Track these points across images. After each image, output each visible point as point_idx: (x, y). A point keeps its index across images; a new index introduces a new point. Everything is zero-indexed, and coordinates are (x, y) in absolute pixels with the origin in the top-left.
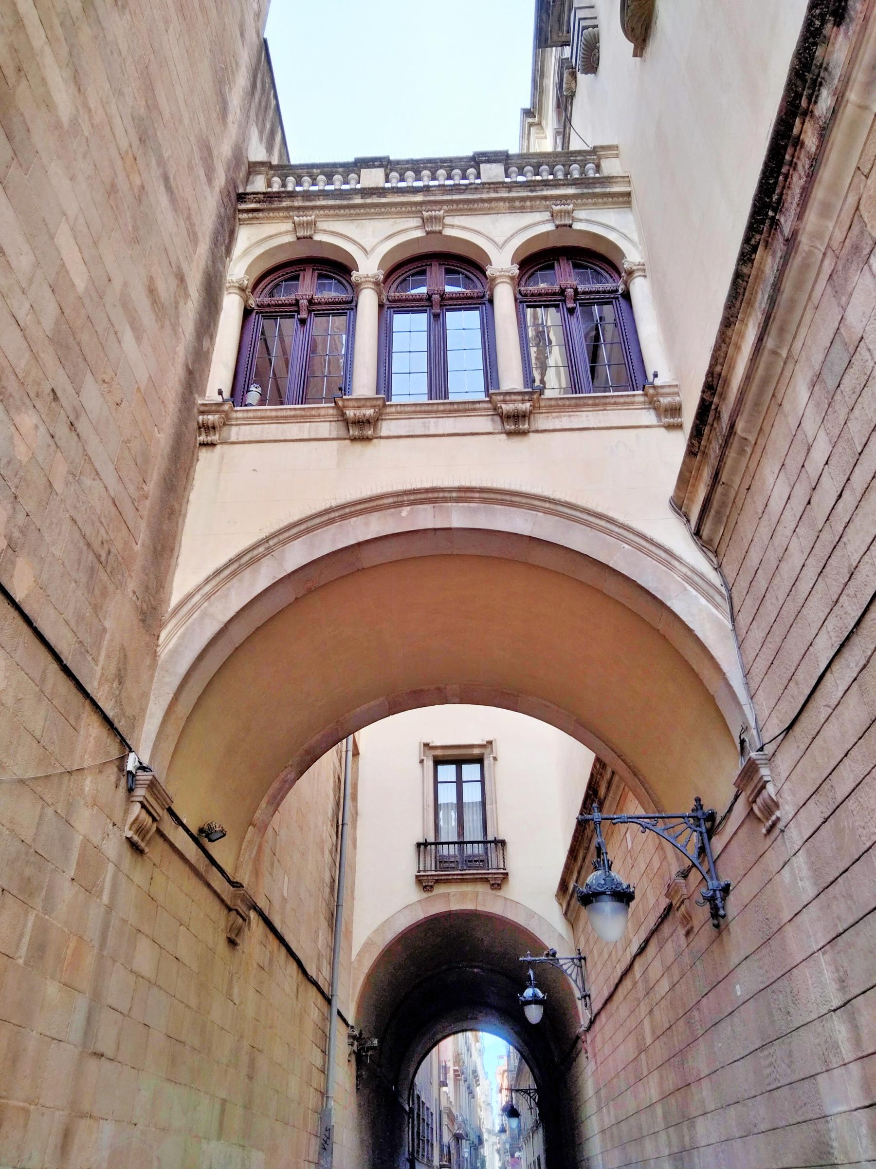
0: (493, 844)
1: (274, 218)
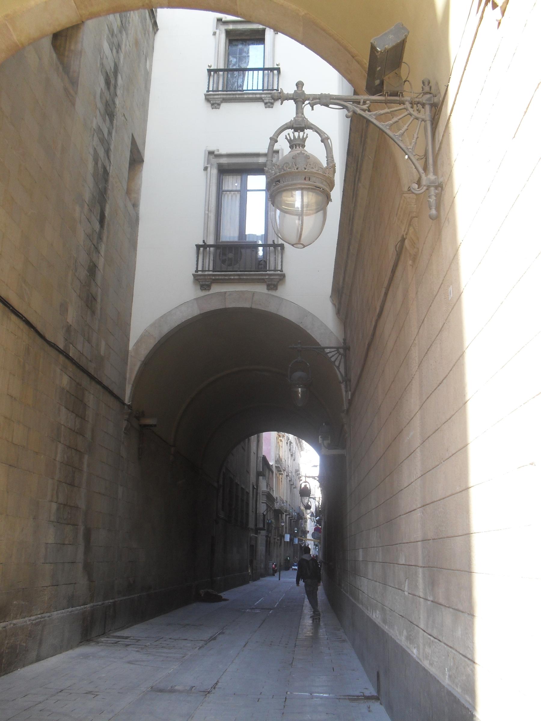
0: (272, 248)
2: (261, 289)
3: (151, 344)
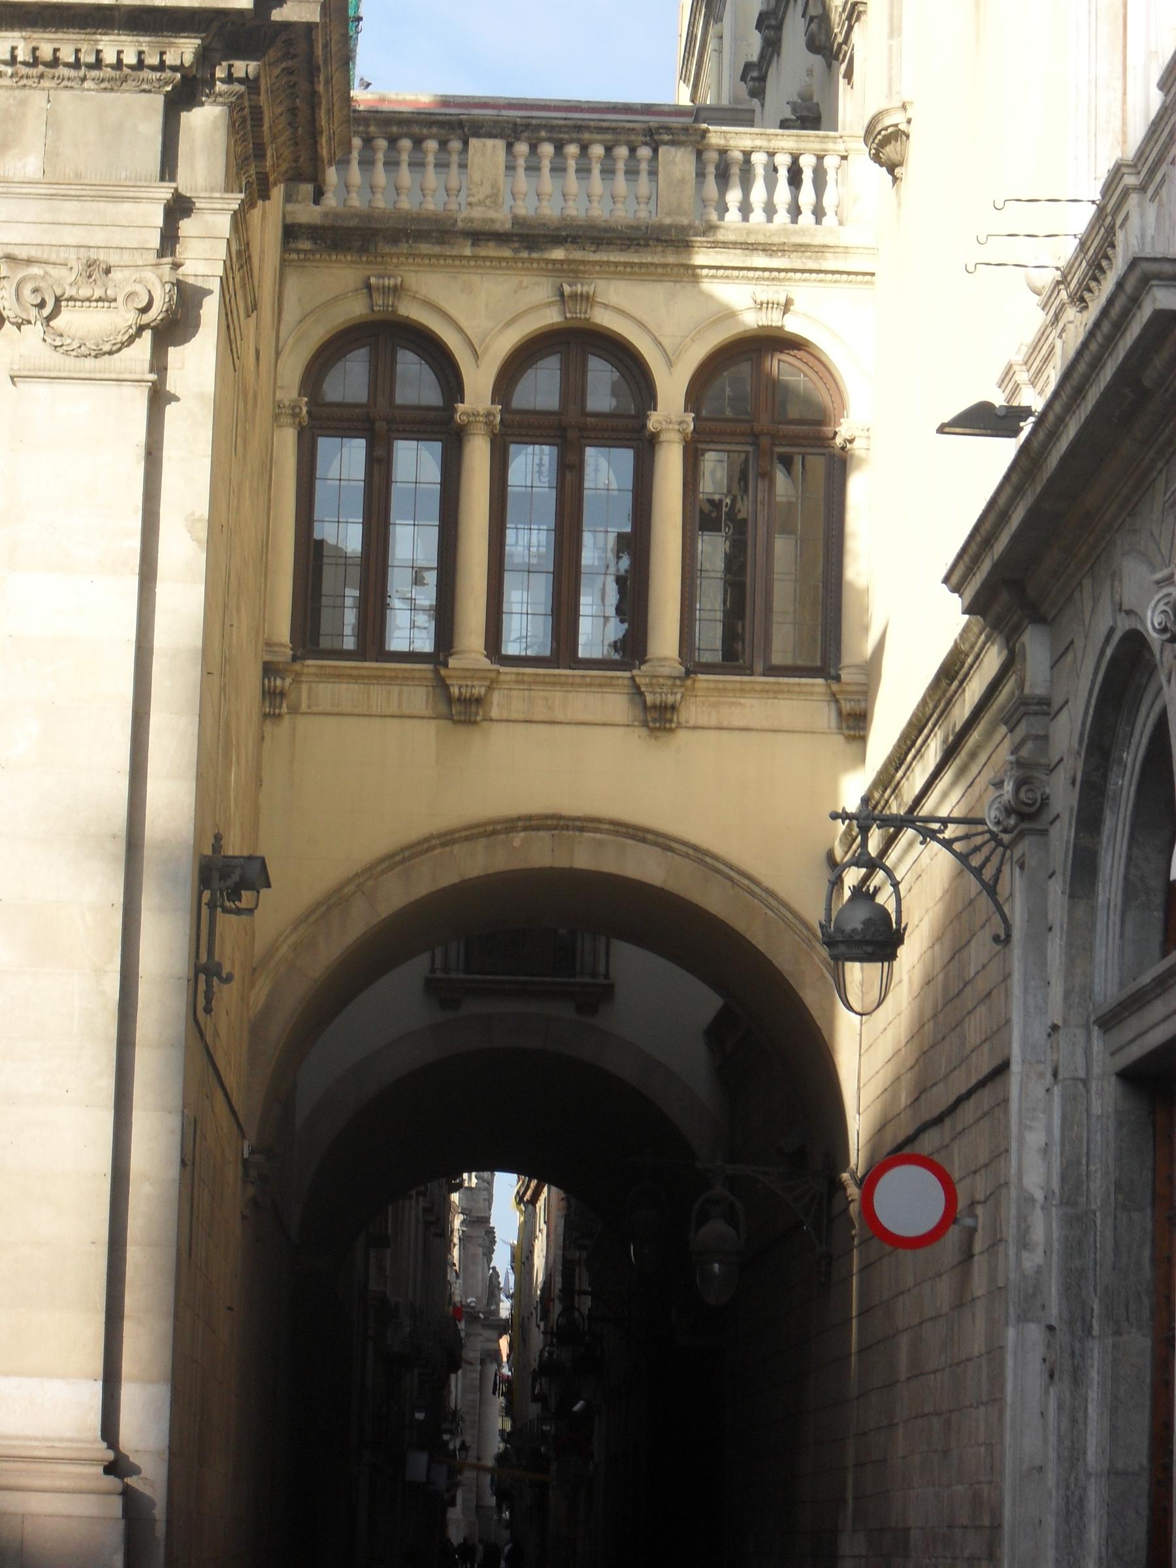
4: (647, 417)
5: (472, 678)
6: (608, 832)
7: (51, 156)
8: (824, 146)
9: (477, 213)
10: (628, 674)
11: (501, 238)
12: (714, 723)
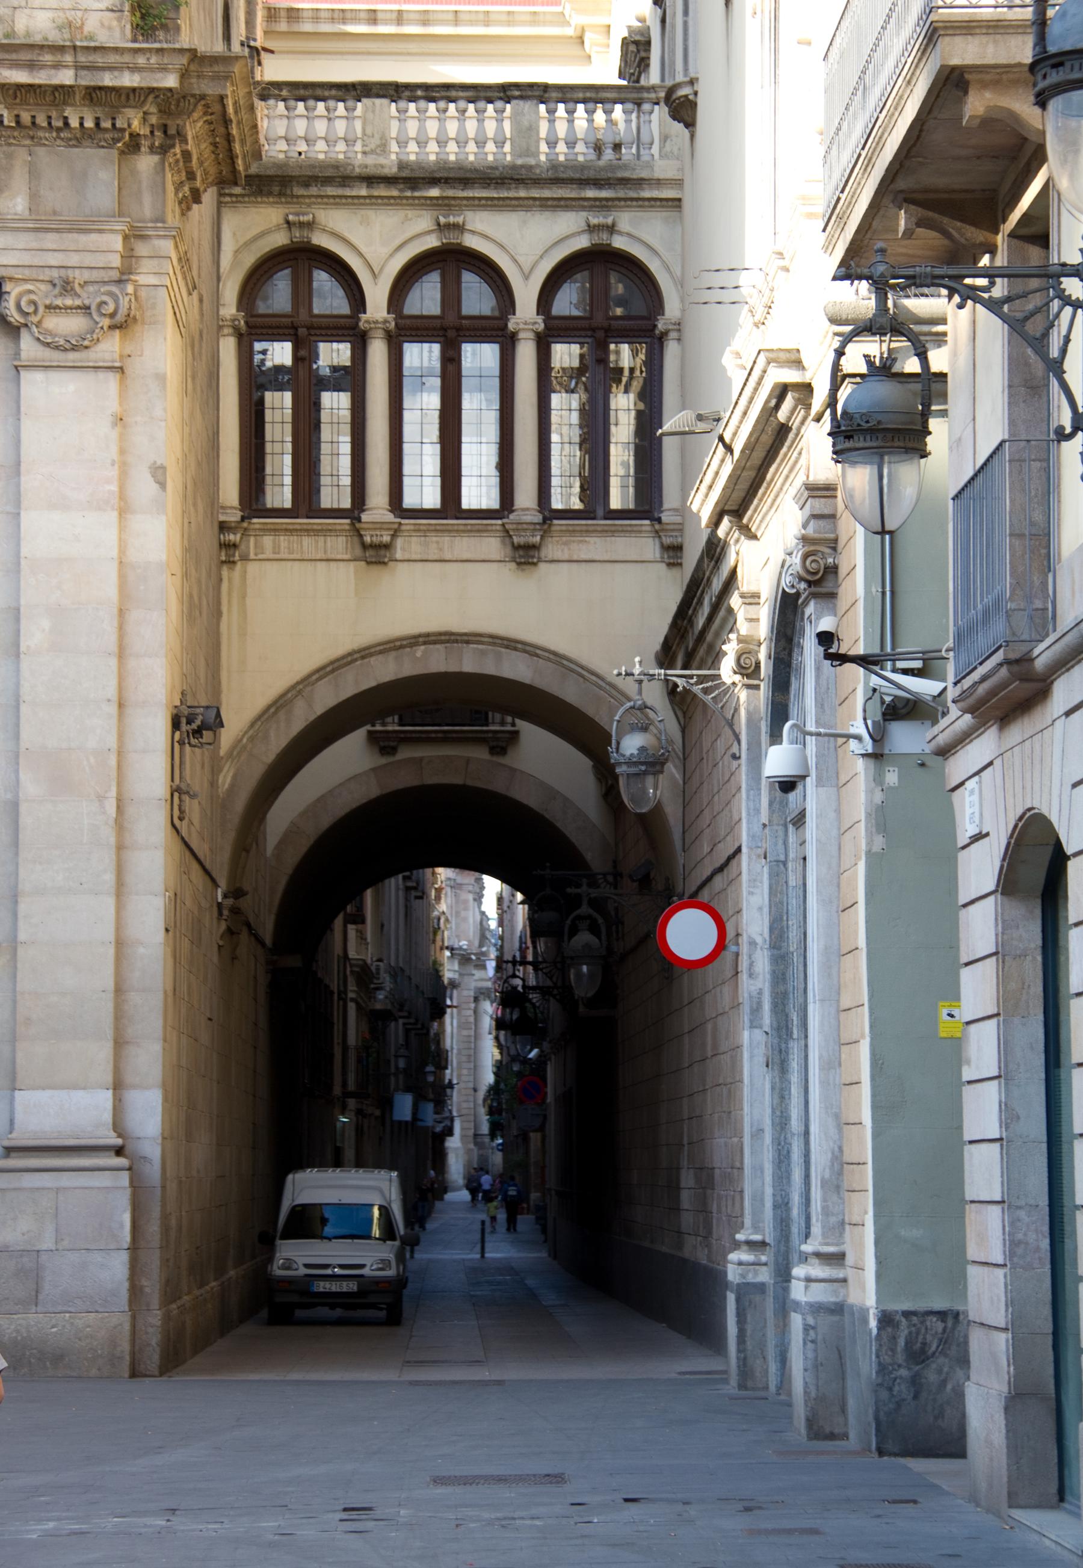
1: (261, 203)
2: (480, 753)
3: (303, 845)
4: (508, 320)
5: (381, 529)
6: (489, 644)
7: (34, 196)
8: (640, 95)
9: (370, 160)
10: (499, 522)
11: (389, 181)
12: (566, 557)
